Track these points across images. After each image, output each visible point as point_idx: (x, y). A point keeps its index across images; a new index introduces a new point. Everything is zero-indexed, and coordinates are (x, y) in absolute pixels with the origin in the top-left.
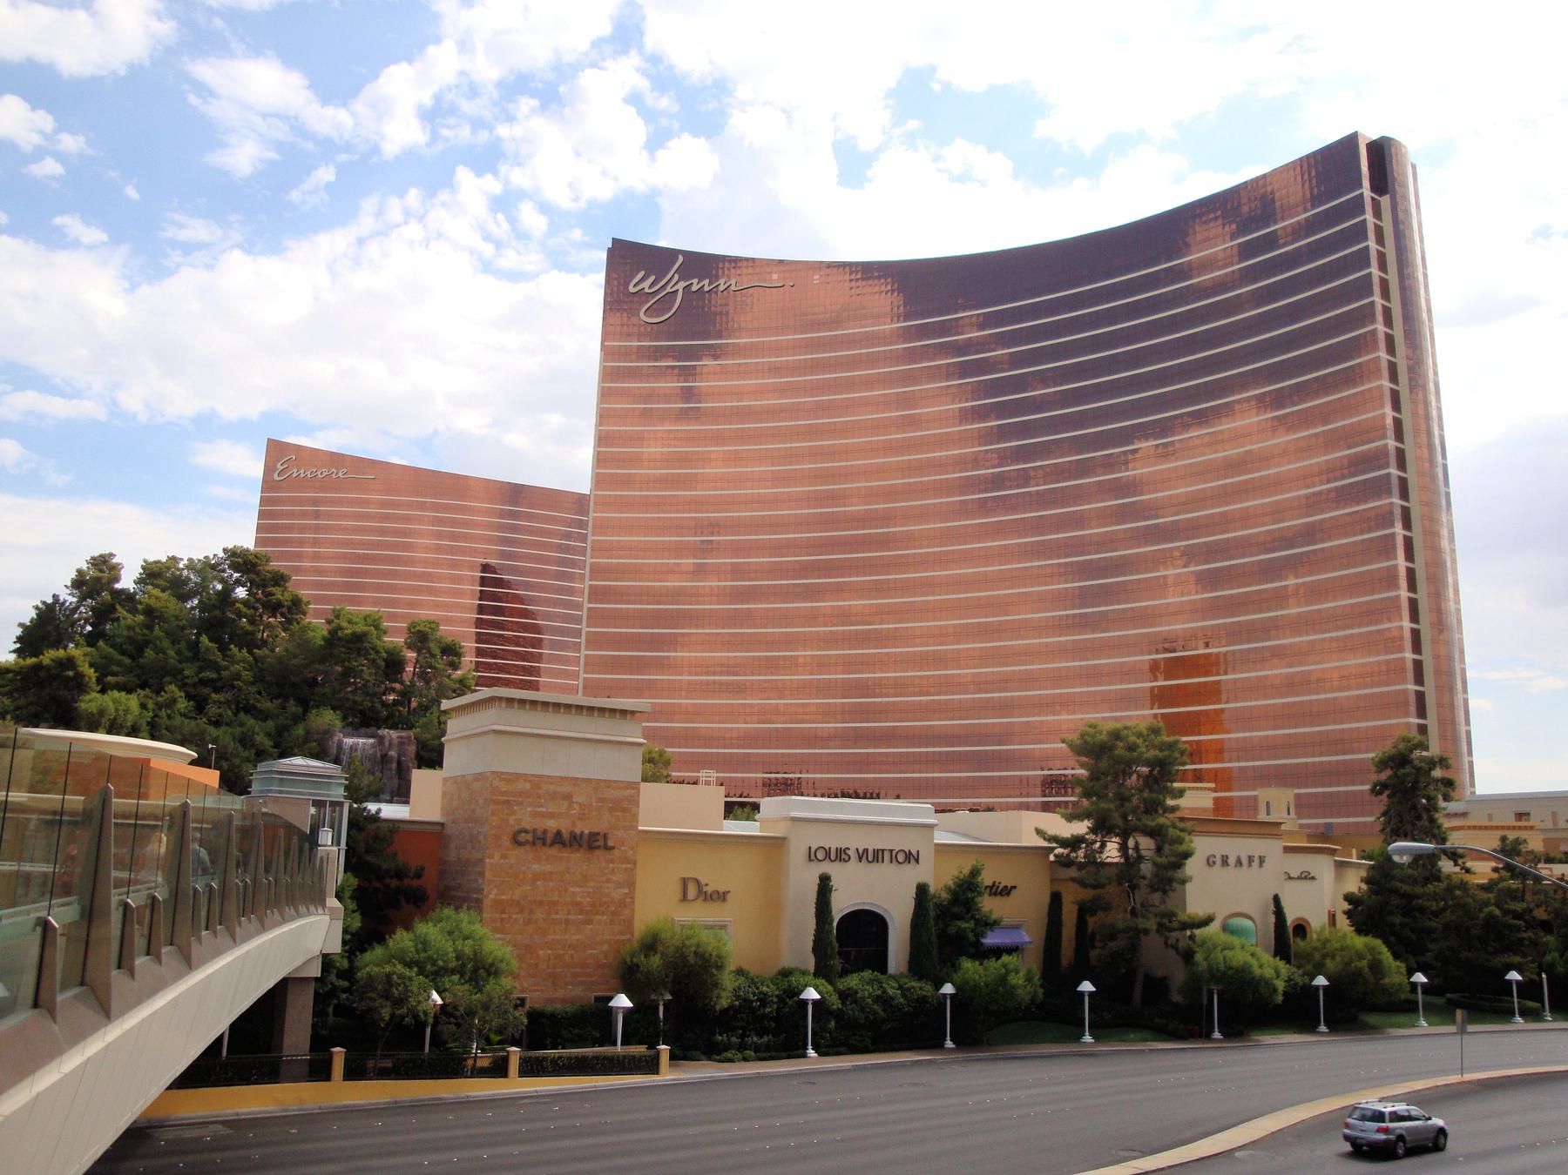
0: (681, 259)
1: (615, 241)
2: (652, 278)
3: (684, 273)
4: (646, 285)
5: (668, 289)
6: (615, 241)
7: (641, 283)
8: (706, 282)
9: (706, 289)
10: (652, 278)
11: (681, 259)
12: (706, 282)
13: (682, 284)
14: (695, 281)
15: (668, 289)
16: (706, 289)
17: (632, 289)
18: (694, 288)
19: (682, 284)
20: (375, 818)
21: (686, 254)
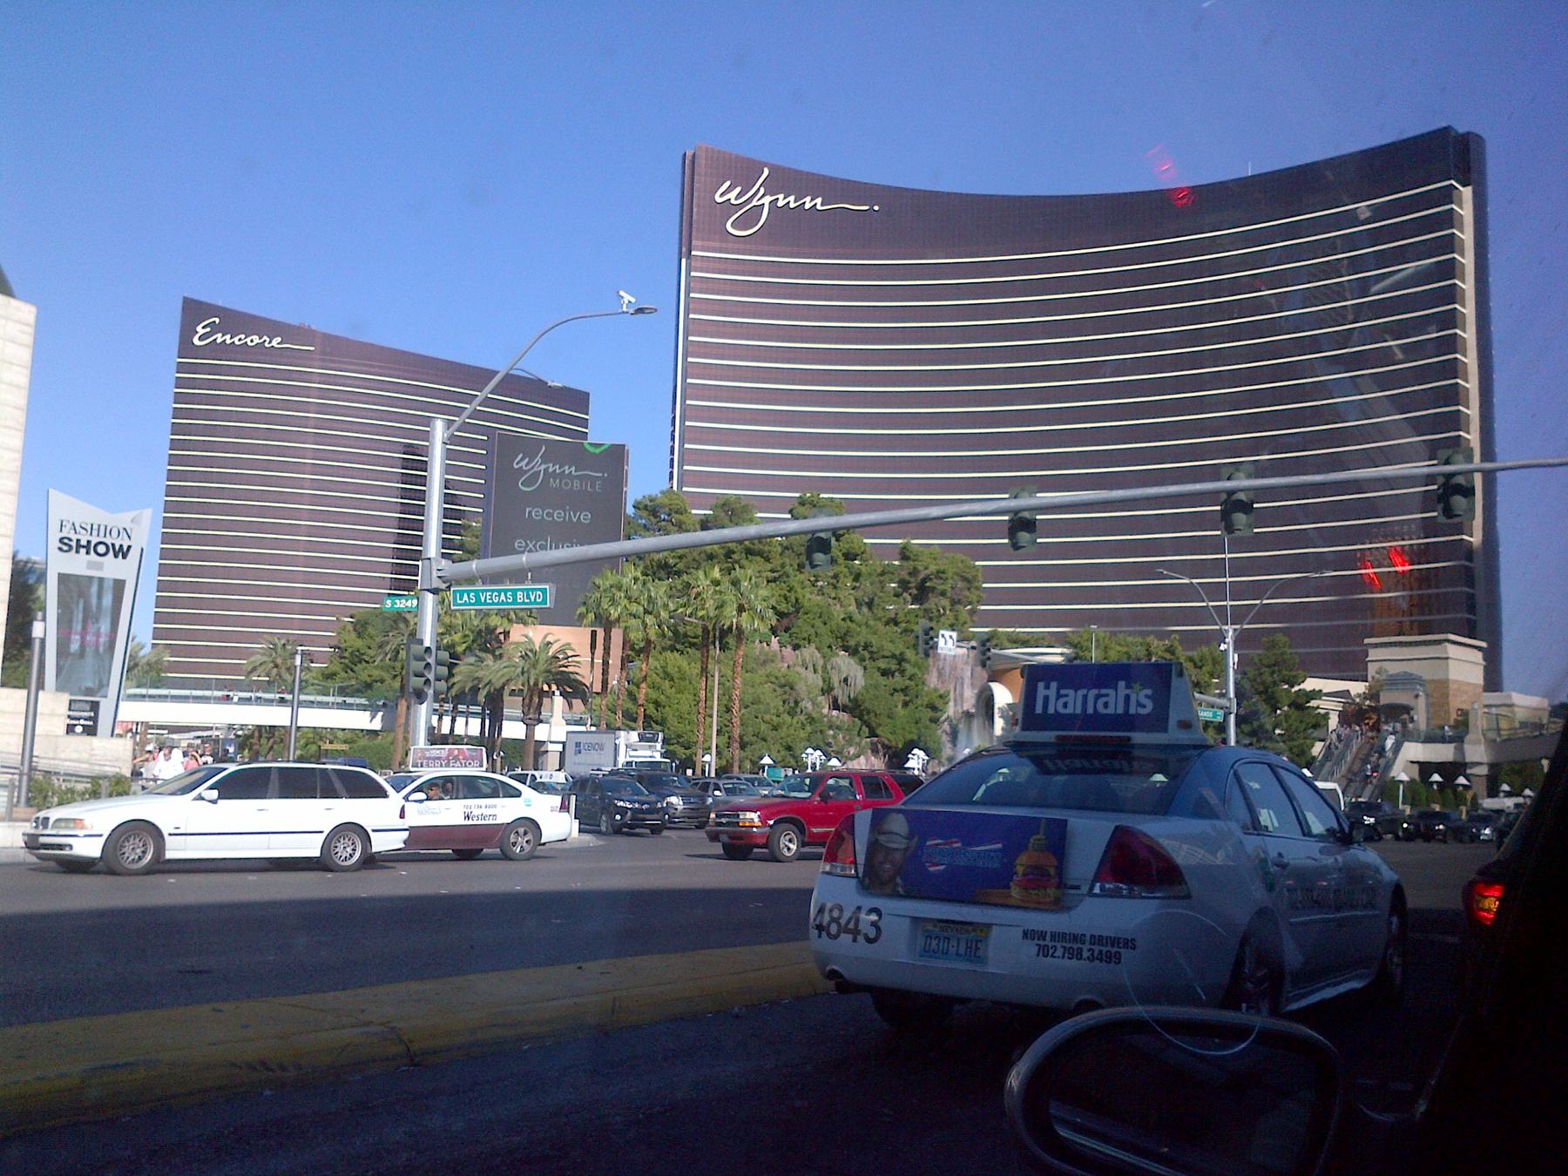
0: (766, 172)
2: (738, 189)
4: (732, 195)
5: (754, 203)
8: (792, 198)
9: (792, 205)
10: (738, 189)
11: (766, 172)
12: (792, 198)
14: (781, 196)
15: (754, 203)
16: (792, 205)
17: (719, 200)
18: (780, 204)
20: (373, 709)
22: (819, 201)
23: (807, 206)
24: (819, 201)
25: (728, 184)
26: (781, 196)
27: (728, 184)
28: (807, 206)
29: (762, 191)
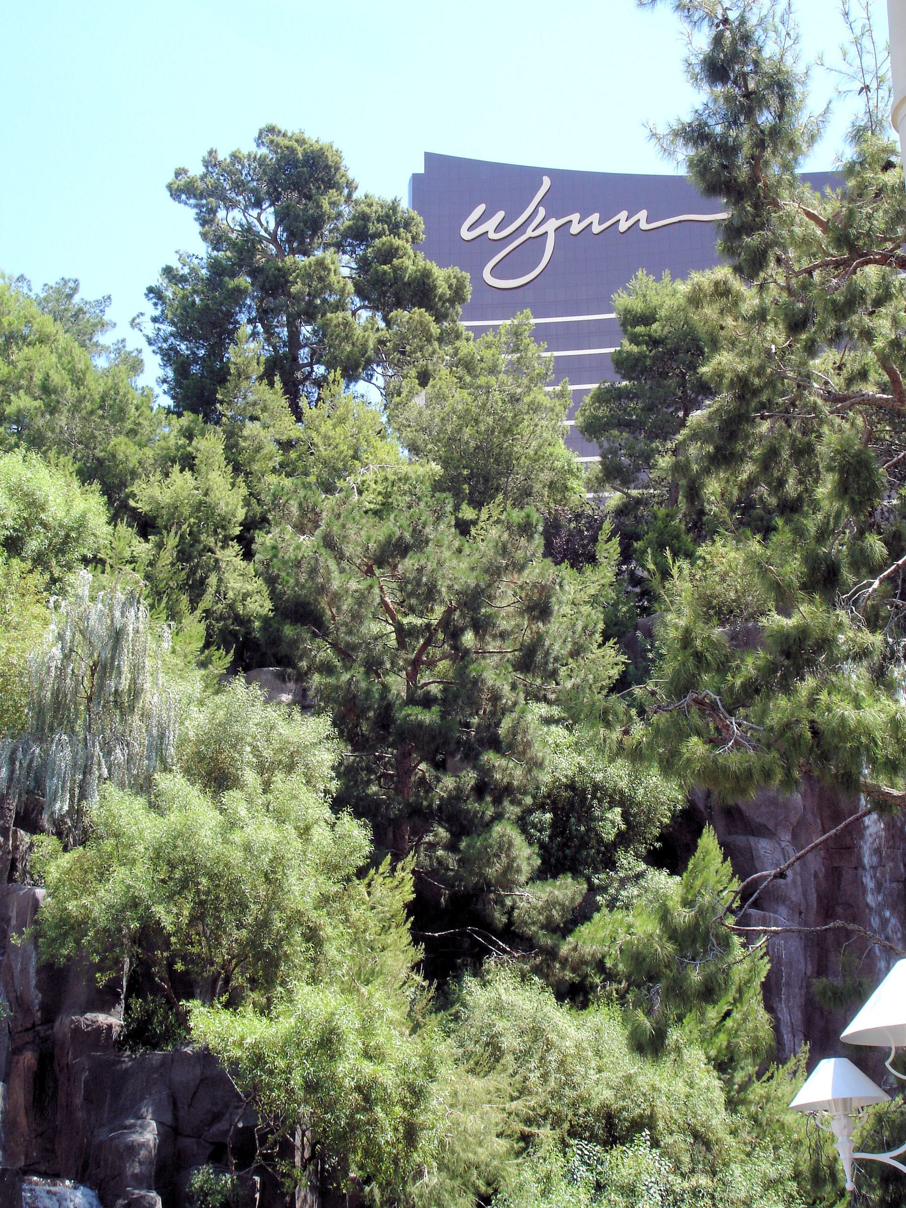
0: (547, 182)
1: (430, 158)
2: (500, 215)
3: (555, 205)
4: (489, 226)
5: (529, 233)
6: (430, 158)
8: (595, 217)
10: (500, 215)
11: (547, 182)
12: (595, 217)
13: (552, 225)
14: (575, 217)
15: (529, 233)
16: (596, 229)
17: (466, 235)
18: (575, 229)
19: (552, 225)
22: (643, 215)
23: (623, 227)
24: (643, 215)
25: (481, 208)
27: (481, 208)
29: (542, 212)
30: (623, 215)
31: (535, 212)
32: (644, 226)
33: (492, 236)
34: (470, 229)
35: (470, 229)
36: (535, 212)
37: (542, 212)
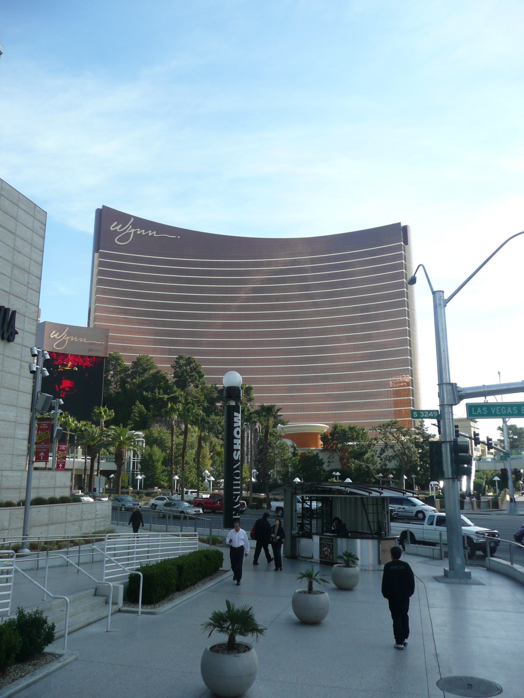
0: (132, 219)
1: (103, 206)
2: (121, 225)
3: (134, 225)
4: (118, 228)
5: (127, 232)
6: (103, 206)
7: (115, 227)
8: (143, 231)
9: (143, 234)
10: (121, 225)
11: (132, 219)
12: (143, 231)
13: (133, 231)
14: (139, 230)
15: (127, 232)
16: (143, 234)
18: (138, 233)
19: (133, 231)
21: (135, 218)
22: (155, 232)
23: (150, 234)
24: (155, 232)
25: (116, 223)
26: (139, 230)
27: (116, 223)
28: (150, 234)
29: (131, 227)
30: (150, 231)
31: (129, 227)
32: (155, 235)
33: (118, 230)
34: (113, 228)
35: (113, 228)
36: (129, 227)
37: (131, 227)
